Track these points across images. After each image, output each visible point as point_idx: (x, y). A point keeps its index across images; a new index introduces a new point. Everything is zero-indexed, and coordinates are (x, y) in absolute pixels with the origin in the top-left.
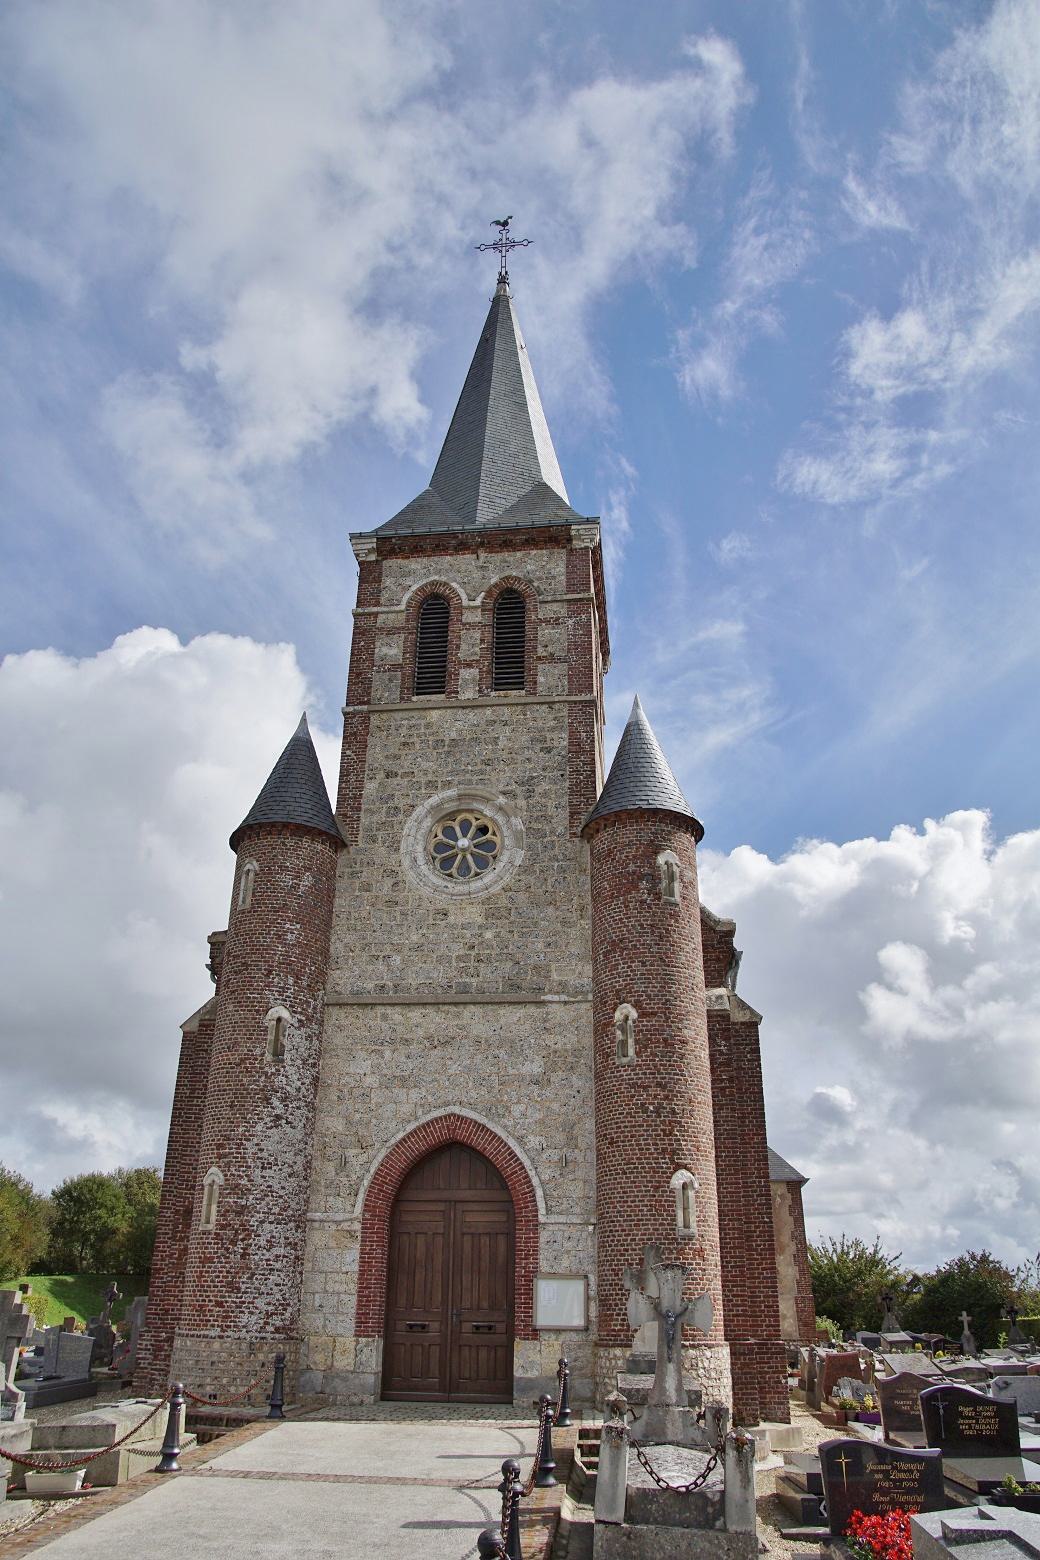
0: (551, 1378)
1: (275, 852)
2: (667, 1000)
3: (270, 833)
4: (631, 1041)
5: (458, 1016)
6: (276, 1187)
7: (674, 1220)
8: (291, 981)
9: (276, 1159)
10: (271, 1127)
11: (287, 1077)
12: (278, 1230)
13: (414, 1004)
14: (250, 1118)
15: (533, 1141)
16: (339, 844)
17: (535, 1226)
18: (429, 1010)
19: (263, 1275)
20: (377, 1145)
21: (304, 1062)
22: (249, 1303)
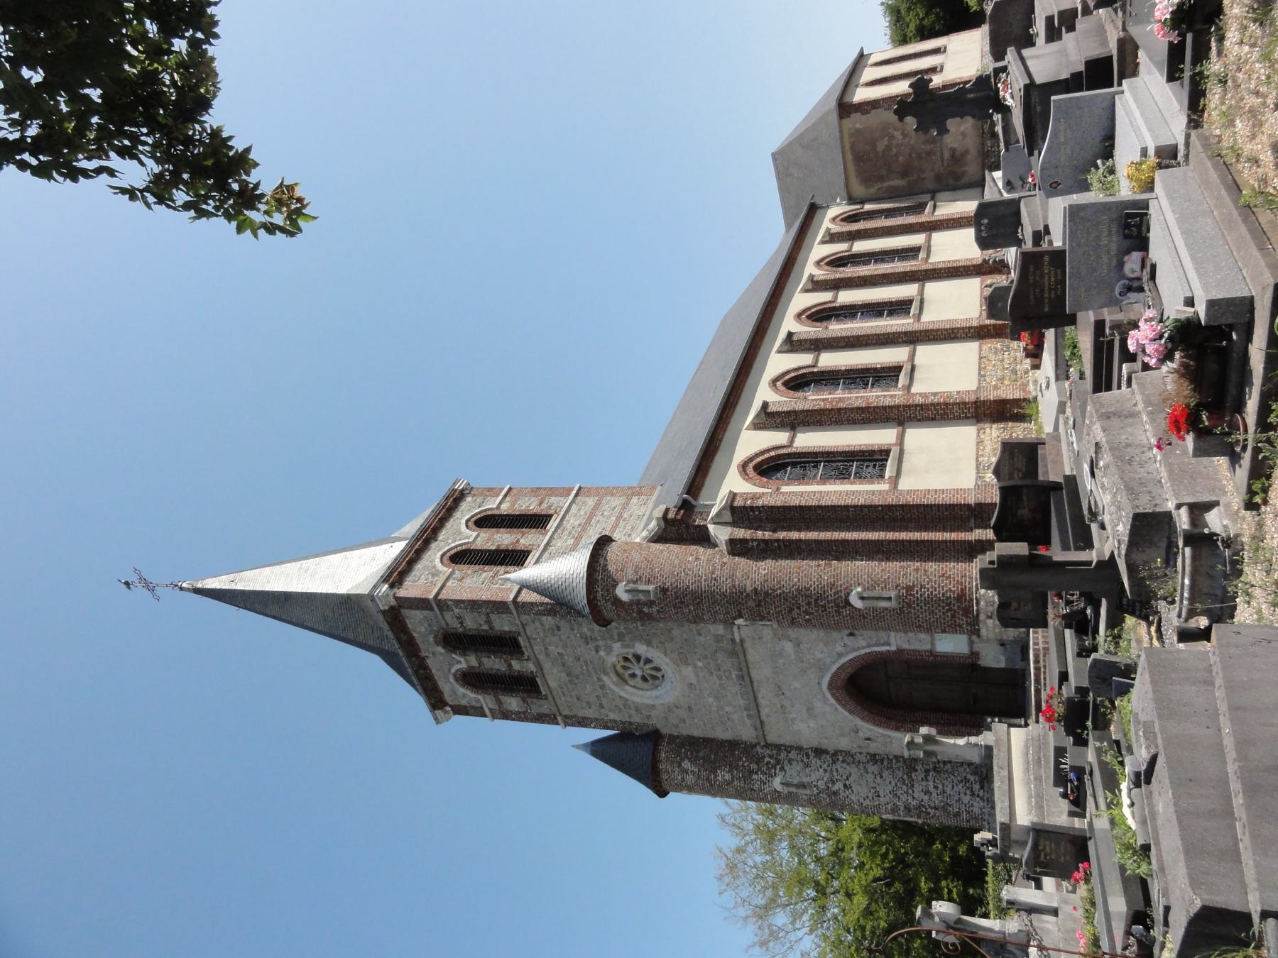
7: (887, 609)
8: (755, 777)
12: (918, 787)
15: (839, 648)
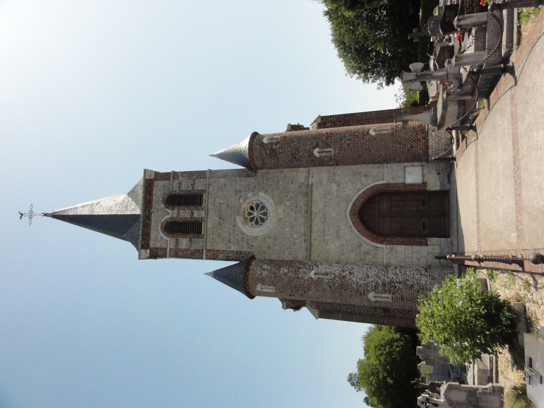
0: (440, 176)
1: (254, 278)
2: (313, 138)
3: (247, 280)
4: (326, 150)
5: (315, 214)
6: (375, 273)
7: (386, 134)
8: (301, 270)
9: (365, 273)
10: (354, 275)
11: (336, 271)
12: (390, 272)
13: (311, 229)
14: (350, 282)
15: (359, 186)
16: (253, 258)
17: (388, 185)
18: (313, 224)
19: (407, 276)
20: (360, 240)
21: (330, 266)
22: (417, 280)
